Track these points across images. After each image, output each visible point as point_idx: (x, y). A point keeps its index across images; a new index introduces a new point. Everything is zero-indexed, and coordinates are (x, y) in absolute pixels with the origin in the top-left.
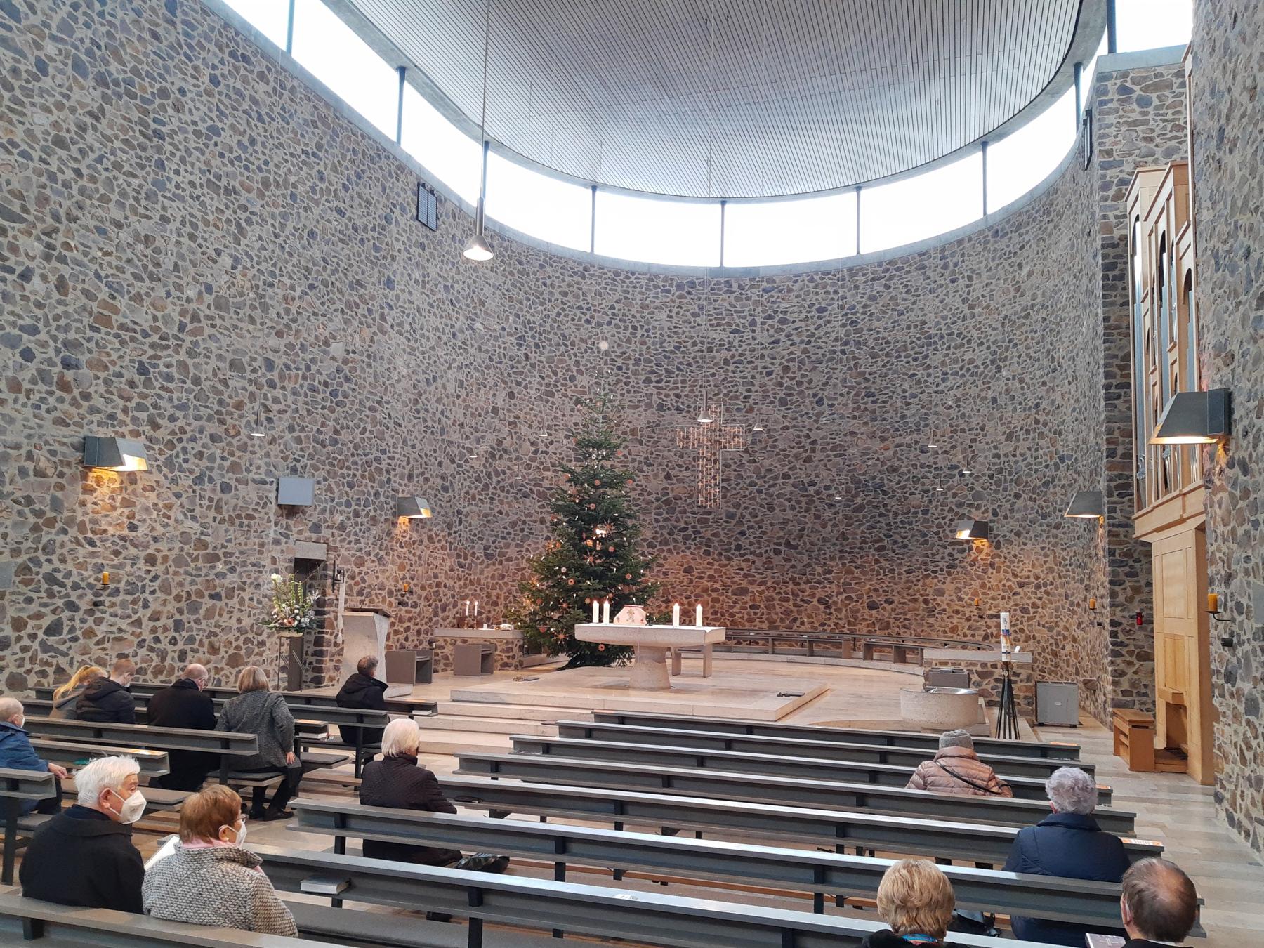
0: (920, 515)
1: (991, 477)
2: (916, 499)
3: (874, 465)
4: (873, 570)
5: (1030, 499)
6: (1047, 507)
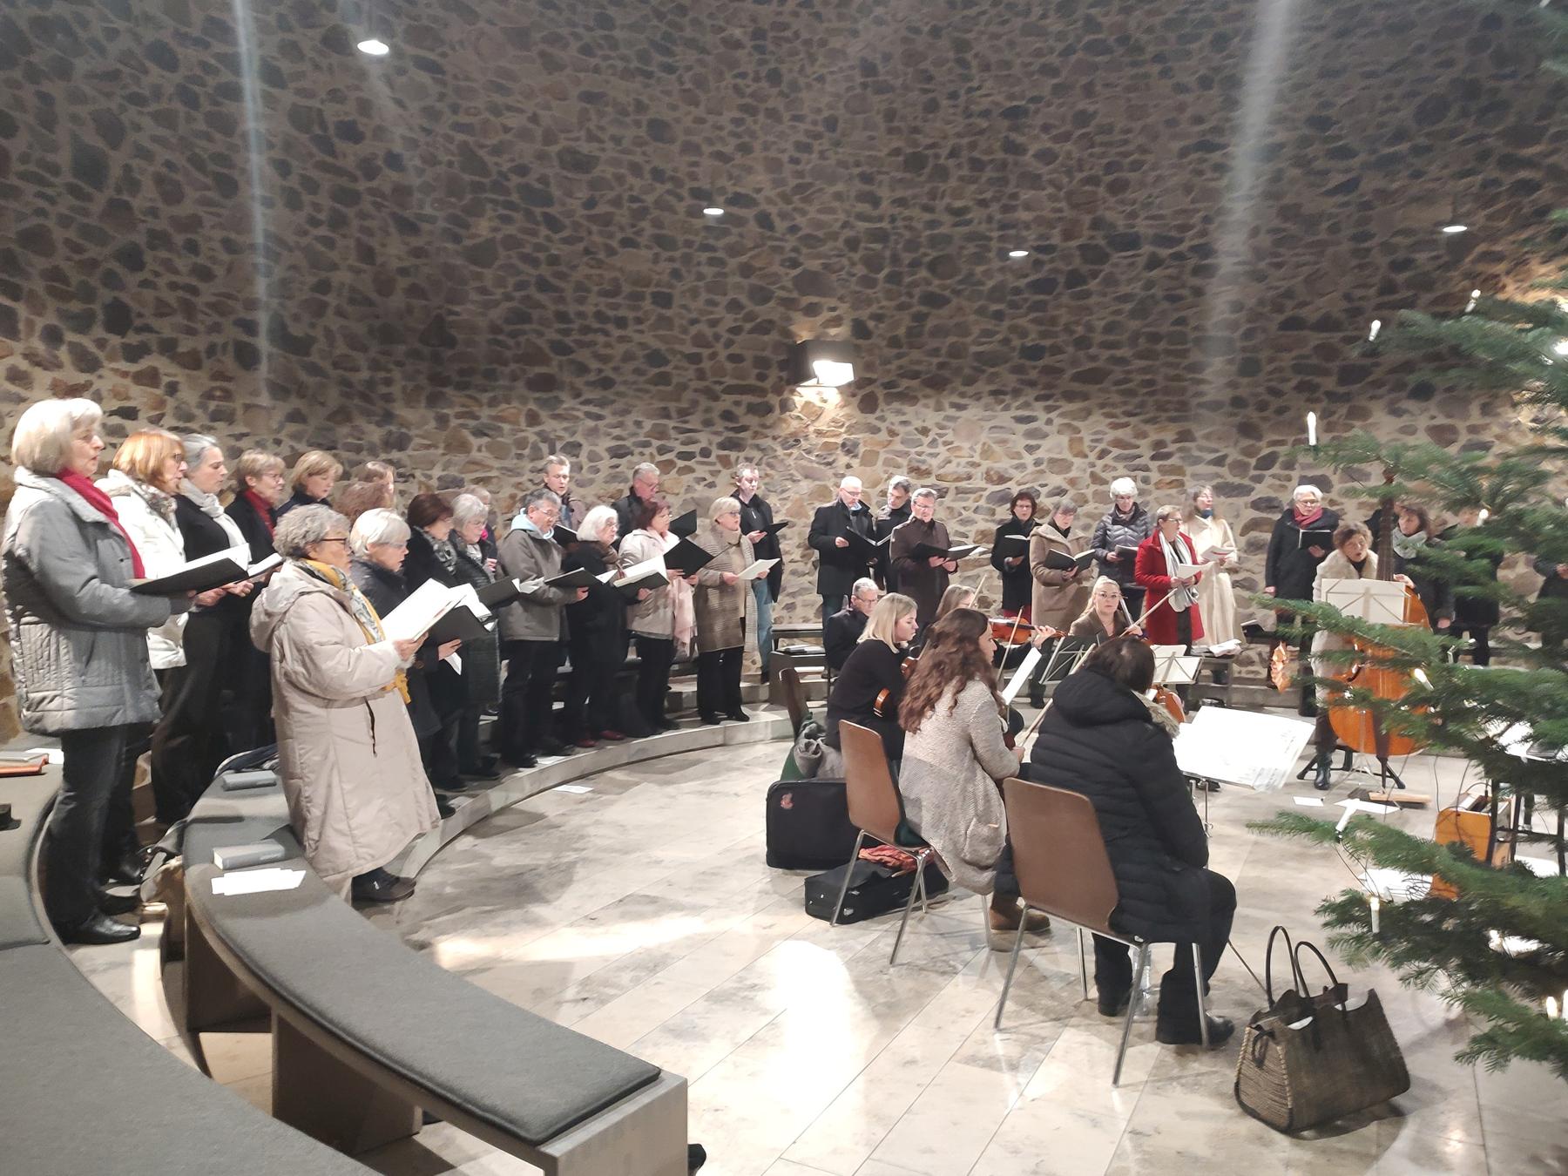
0: (647, 304)
1: (852, 244)
2: (640, 261)
3: (524, 134)
4: (521, 444)
5: (981, 311)
6: (1044, 335)
